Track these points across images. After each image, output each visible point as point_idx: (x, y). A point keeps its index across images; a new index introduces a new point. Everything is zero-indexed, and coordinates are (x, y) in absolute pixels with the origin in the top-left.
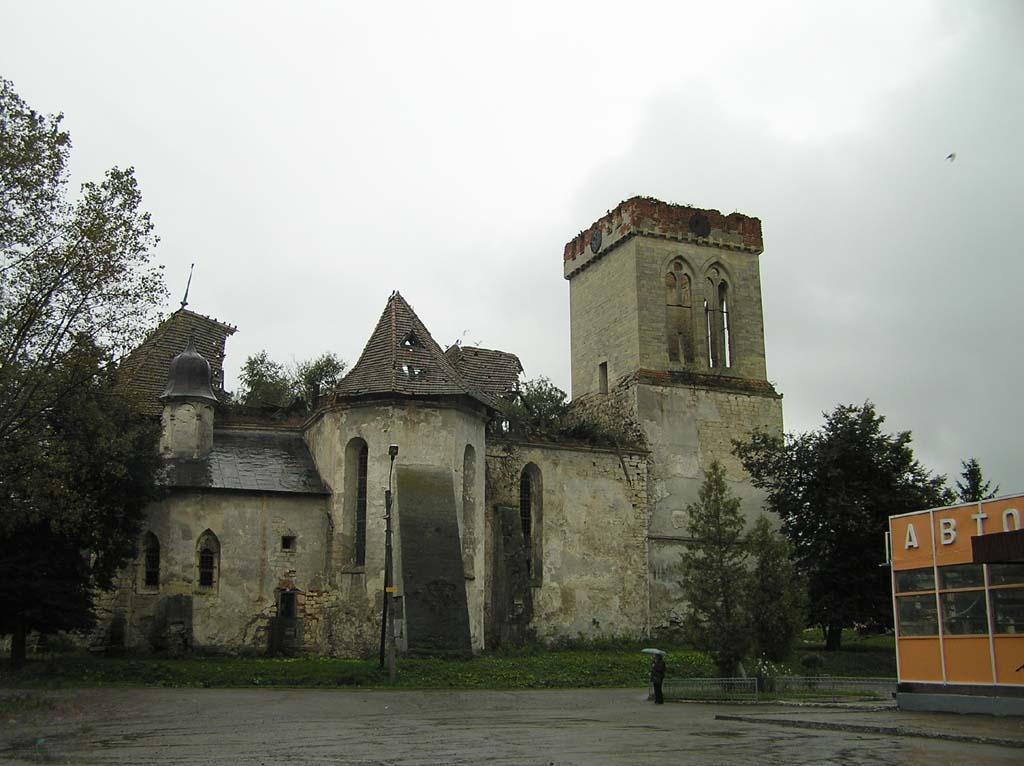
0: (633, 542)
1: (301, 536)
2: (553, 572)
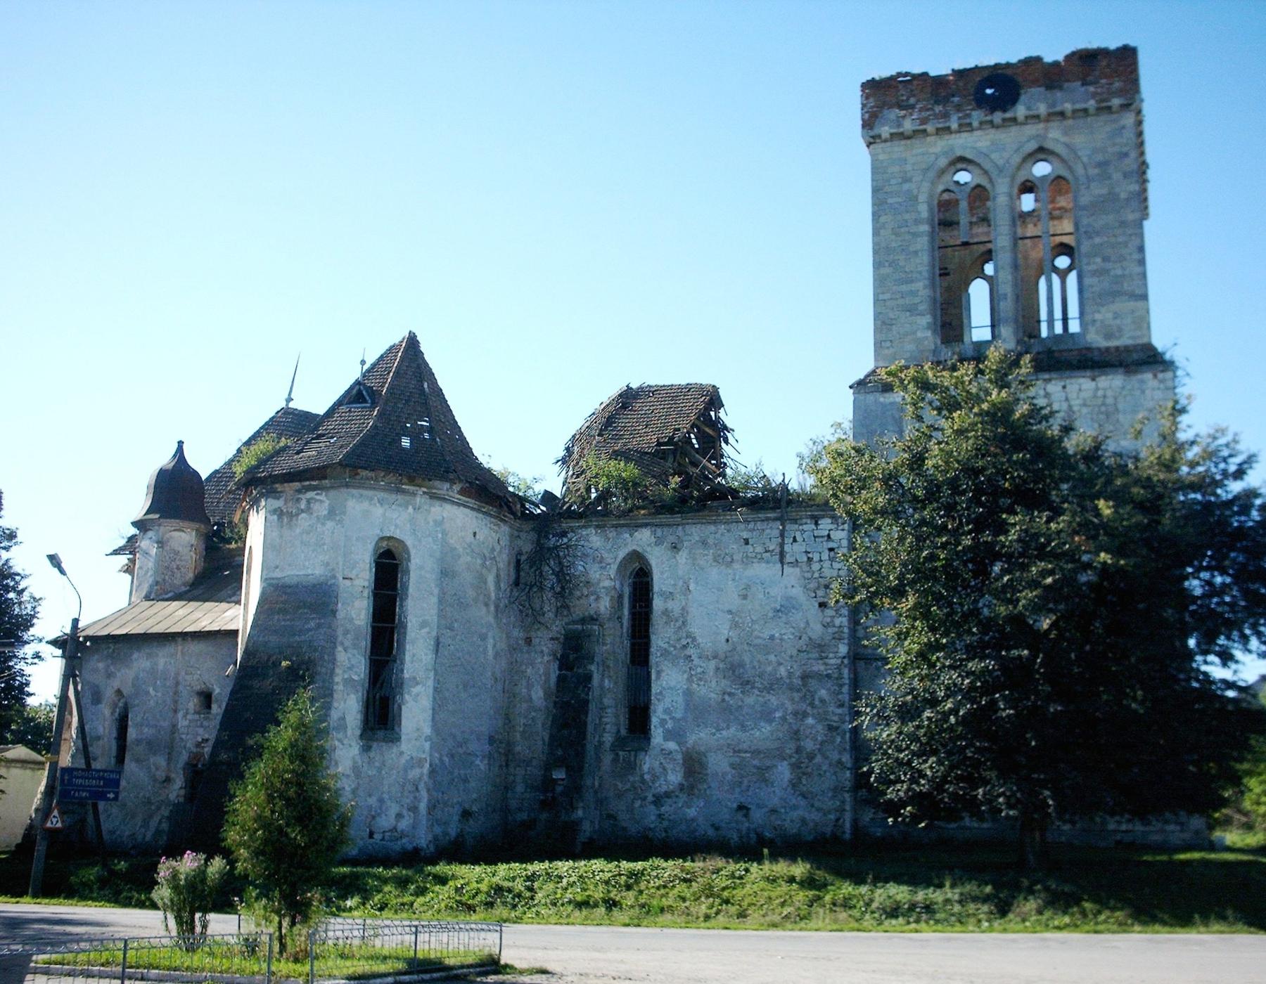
0: (819, 667)
2: (670, 725)
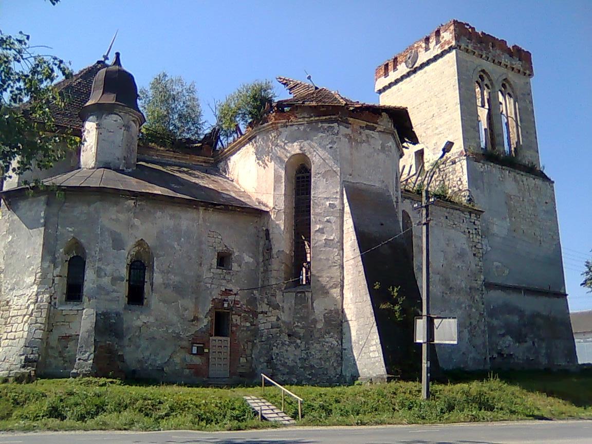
1: (236, 254)
